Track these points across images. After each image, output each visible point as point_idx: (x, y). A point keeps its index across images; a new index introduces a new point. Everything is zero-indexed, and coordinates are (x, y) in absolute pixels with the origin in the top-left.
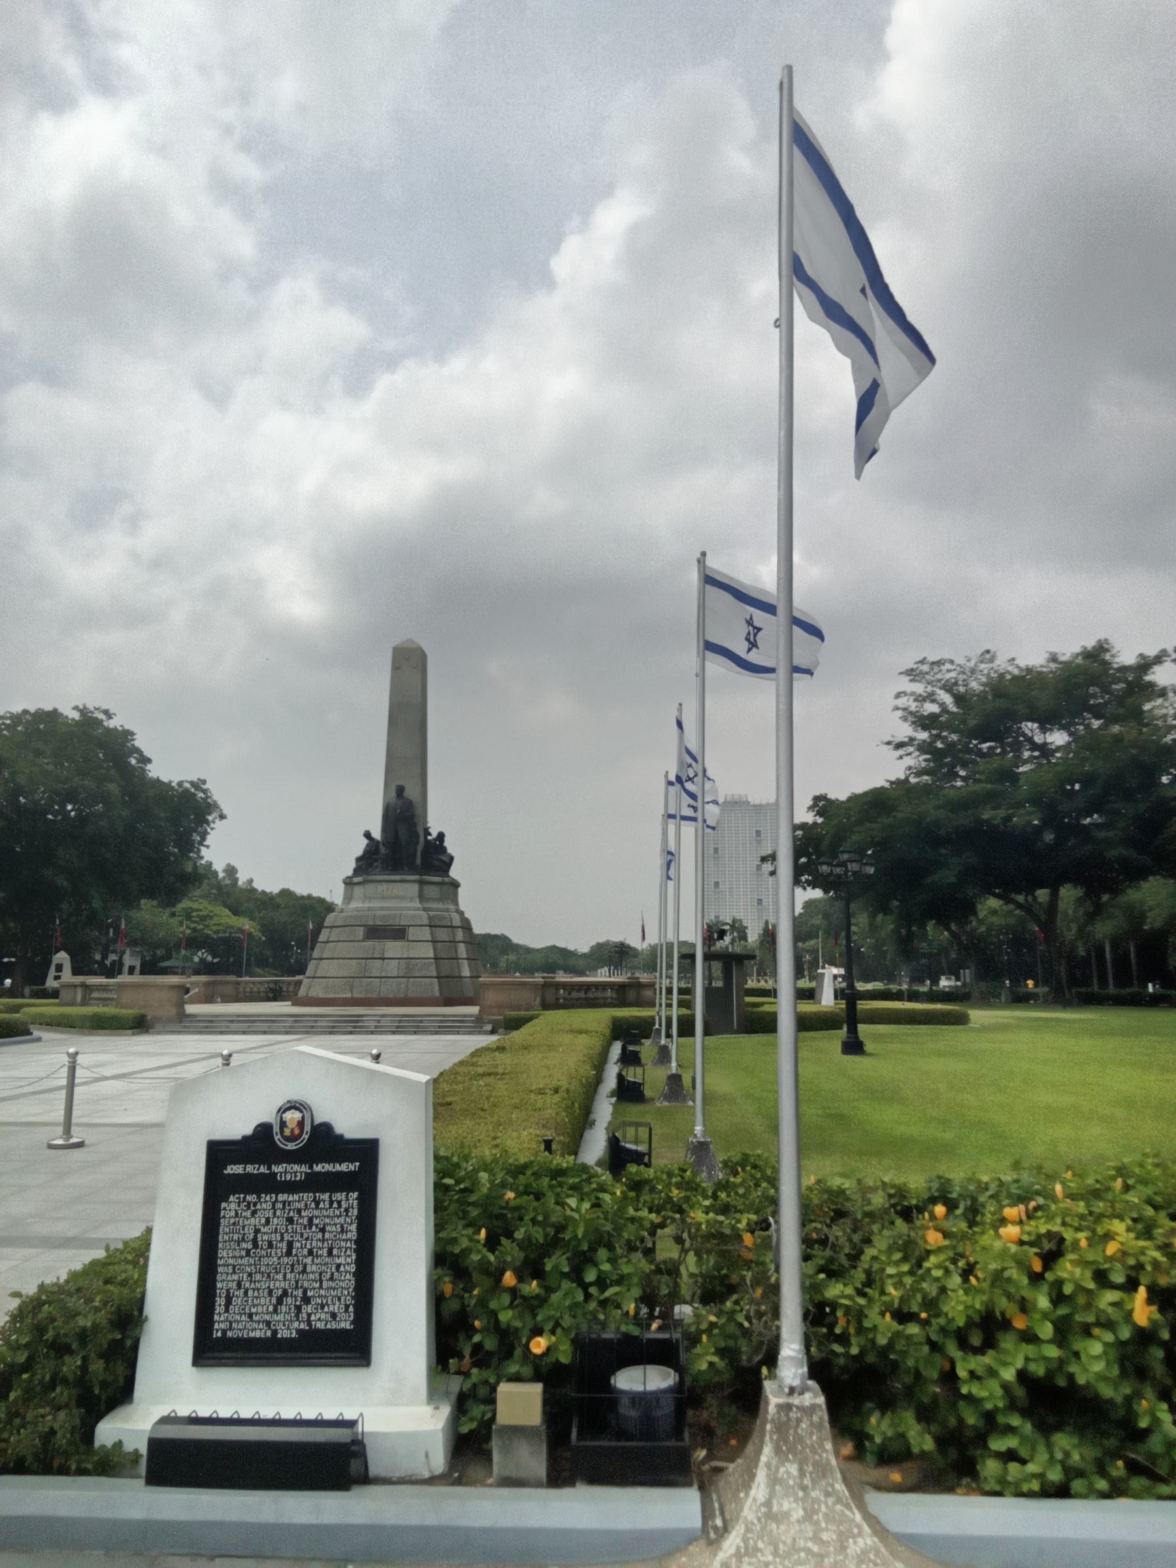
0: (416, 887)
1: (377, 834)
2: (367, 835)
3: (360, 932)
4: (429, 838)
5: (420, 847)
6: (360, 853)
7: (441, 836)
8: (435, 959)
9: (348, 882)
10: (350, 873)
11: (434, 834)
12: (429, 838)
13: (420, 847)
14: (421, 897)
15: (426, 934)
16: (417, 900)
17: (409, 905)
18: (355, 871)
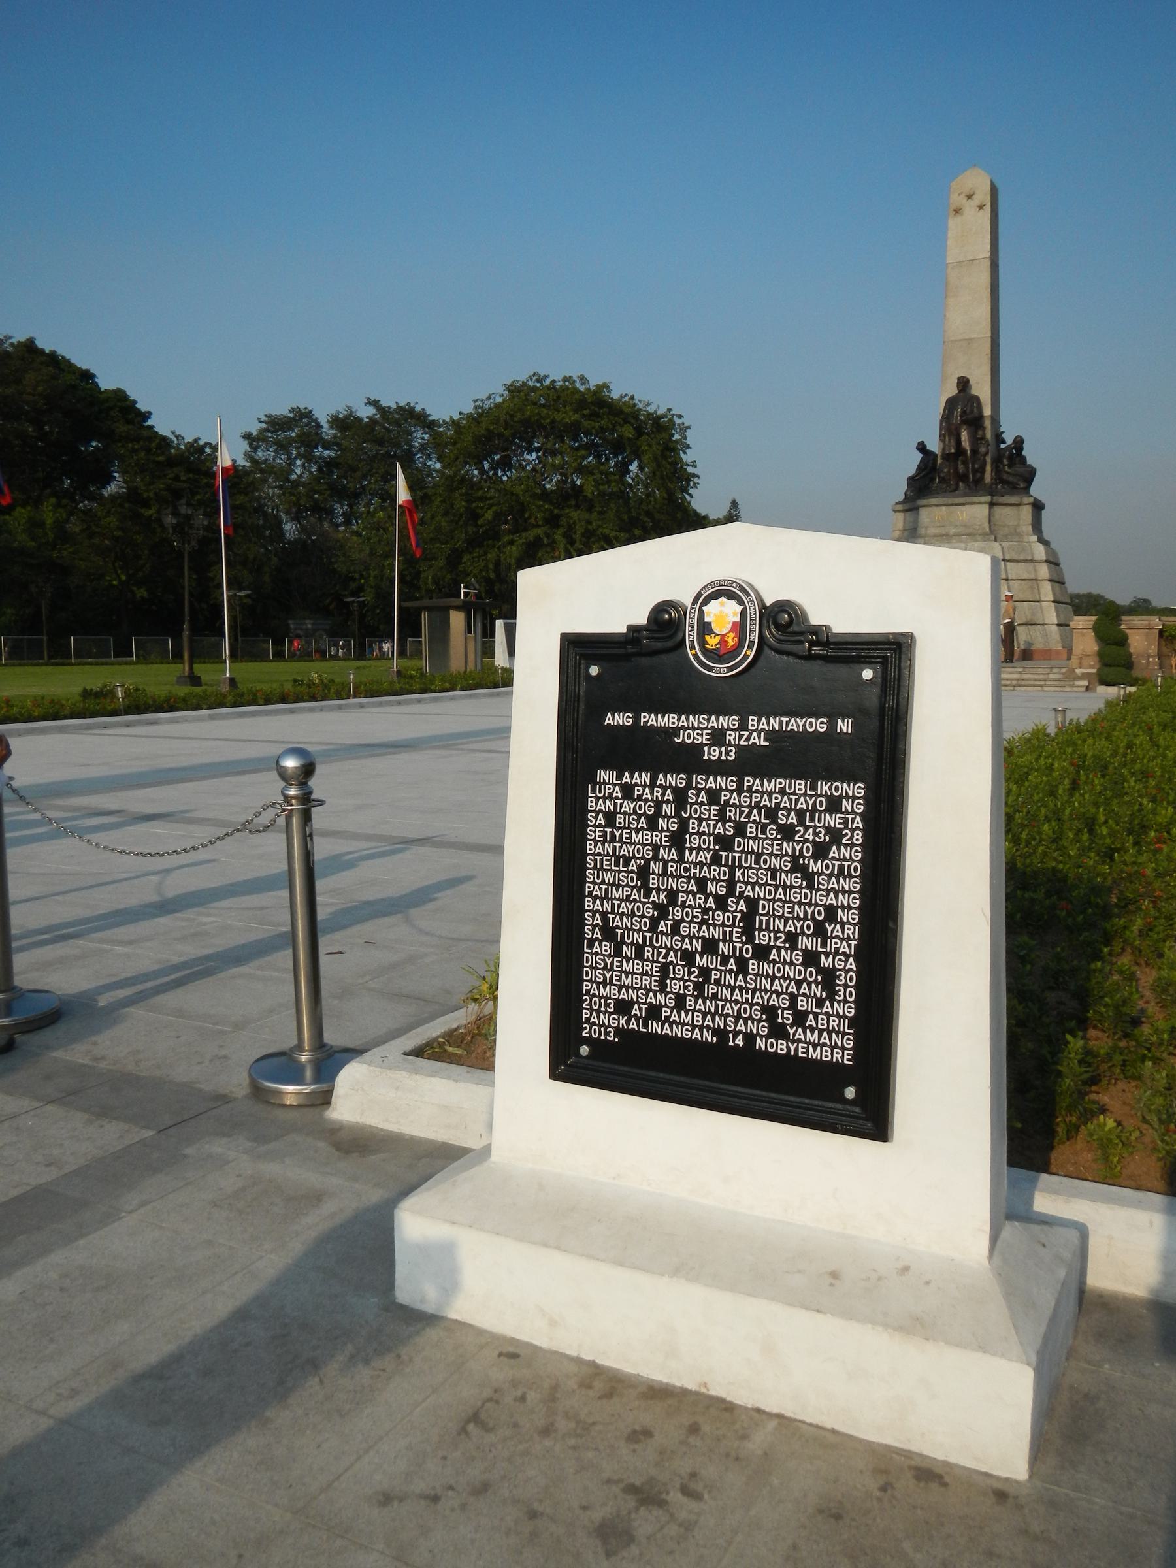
0: (986, 508)
2: (922, 447)
4: (1003, 446)
6: (912, 471)
7: (1019, 443)
11: (1009, 439)
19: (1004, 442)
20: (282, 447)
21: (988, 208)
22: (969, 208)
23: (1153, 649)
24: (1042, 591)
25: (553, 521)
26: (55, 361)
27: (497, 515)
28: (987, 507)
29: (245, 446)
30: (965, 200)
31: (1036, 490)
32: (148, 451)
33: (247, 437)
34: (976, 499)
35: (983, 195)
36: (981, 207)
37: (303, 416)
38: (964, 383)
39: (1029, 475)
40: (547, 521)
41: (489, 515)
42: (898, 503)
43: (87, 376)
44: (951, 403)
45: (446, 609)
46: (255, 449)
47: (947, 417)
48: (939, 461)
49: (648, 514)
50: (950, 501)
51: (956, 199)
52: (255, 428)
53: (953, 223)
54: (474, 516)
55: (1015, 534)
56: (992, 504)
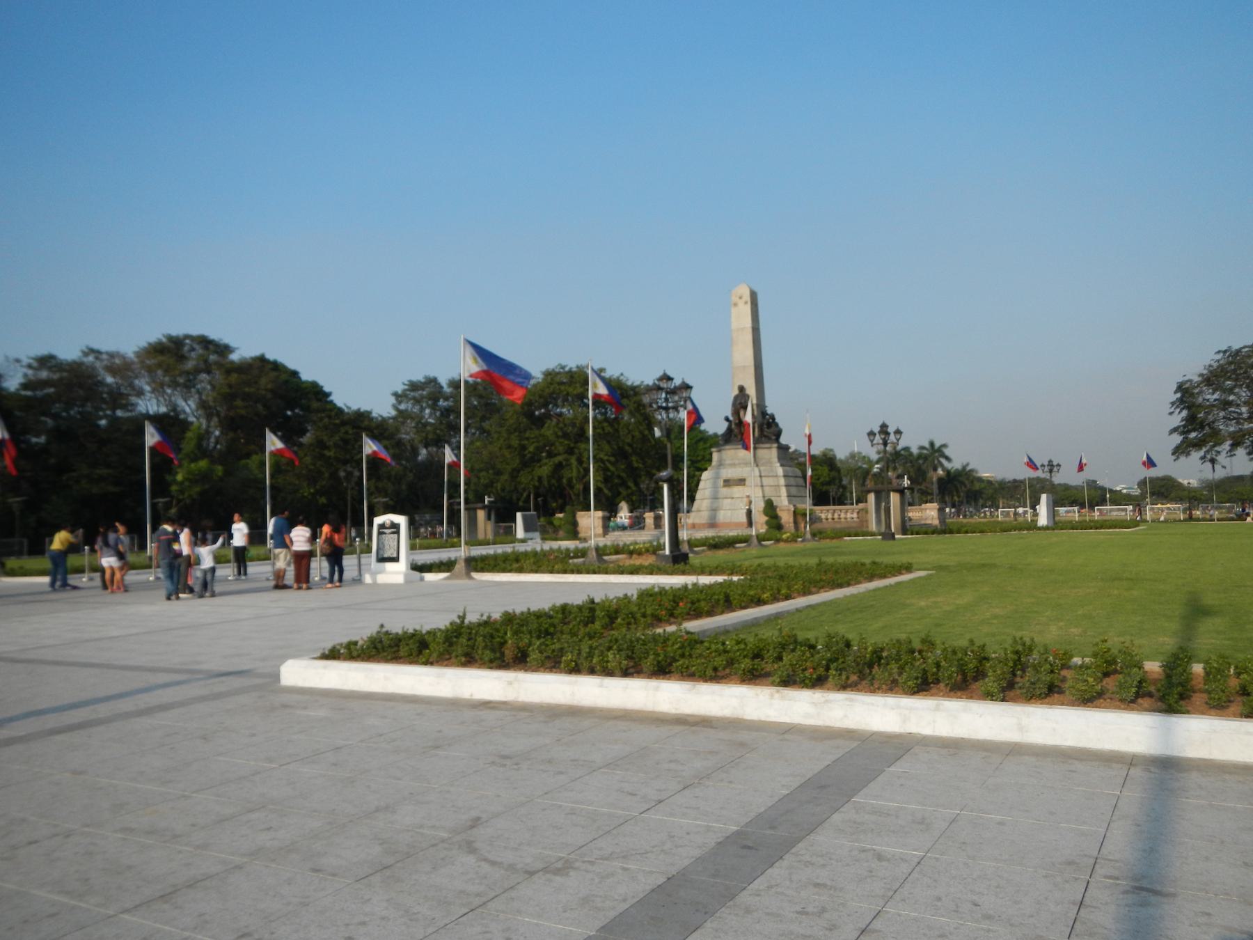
2: (727, 419)
20: (417, 401)
22: (741, 303)
23: (791, 520)
25: (570, 451)
26: (276, 366)
27: (537, 448)
29: (393, 400)
31: (783, 440)
32: (330, 417)
33: (396, 395)
35: (747, 297)
37: (432, 382)
38: (742, 389)
39: (778, 434)
40: (566, 452)
41: (531, 449)
43: (295, 374)
44: (736, 398)
45: (475, 509)
46: (400, 403)
47: (734, 405)
49: (630, 445)
51: (734, 299)
52: (400, 388)
53: (734, 311)
54: (524, 448)
55: (769, 462)
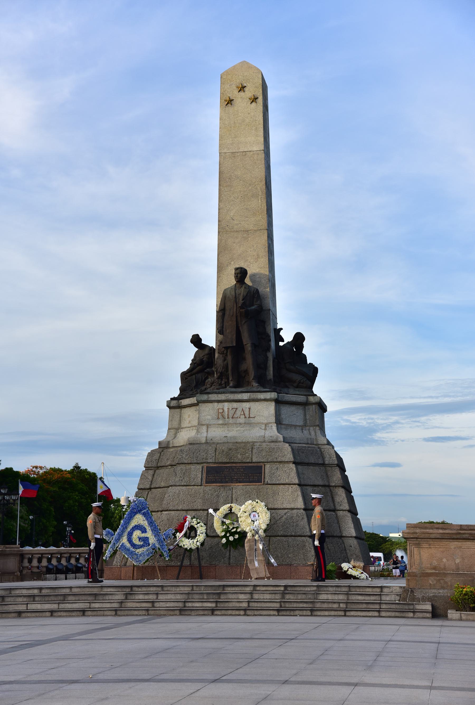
0: (271, 407)
1: (210, 339)
2: (196, 340)
3: (197, 473)
4: (281, 344)
5: (271, 356)
8: (304, 509)
9: (175, 405)
10: (176, 393)
11: (287, 336)
12: (281, 344)
13: (271, 356)
14: (279, 422)
15: (290, 473)
16: (274, 427)
17: (262, 433)
18: (181, 389)
19: (283, 341)
21: (260, 100)
24: (338, 499)
28: (273, 404)
30: (236, 92)
34: (262, 396)
36: (254, 100)
38: (241, 274)
42: (171, 399)
48: (217, 355)
50: (231, 396)
56: (278, 402)
